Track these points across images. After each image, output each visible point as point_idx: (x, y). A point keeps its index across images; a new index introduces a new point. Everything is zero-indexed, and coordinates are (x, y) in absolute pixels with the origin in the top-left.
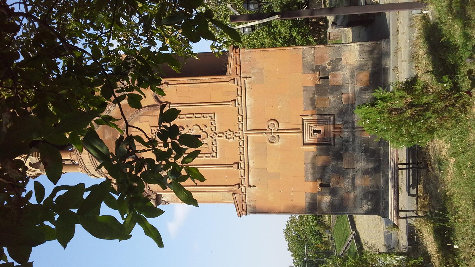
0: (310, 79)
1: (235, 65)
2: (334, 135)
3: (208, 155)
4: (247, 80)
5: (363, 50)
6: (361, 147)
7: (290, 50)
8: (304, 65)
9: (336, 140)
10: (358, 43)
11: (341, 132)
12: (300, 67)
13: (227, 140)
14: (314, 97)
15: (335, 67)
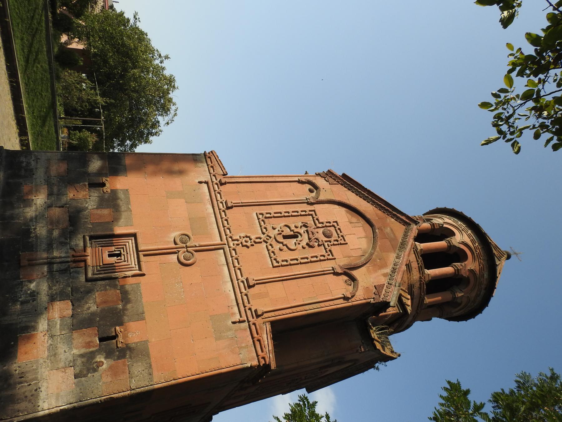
0: (133, 333)
1: (261, 338)
2: (85, 249)
3: (268, 215)
4: (237, 318)
5: (30, 401)
6: (36, 236)
7: (176, 377)
8: (148, 355)
9: (81, 244)
10: (41, 413)
11: (73, 256)
12: (153, 352)
13: (248, 235)
14: (124, 306)
15: (88, 360)
